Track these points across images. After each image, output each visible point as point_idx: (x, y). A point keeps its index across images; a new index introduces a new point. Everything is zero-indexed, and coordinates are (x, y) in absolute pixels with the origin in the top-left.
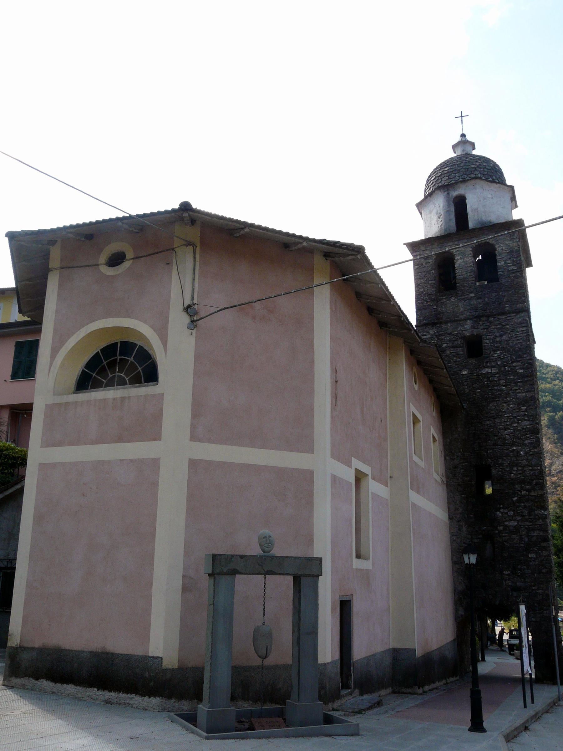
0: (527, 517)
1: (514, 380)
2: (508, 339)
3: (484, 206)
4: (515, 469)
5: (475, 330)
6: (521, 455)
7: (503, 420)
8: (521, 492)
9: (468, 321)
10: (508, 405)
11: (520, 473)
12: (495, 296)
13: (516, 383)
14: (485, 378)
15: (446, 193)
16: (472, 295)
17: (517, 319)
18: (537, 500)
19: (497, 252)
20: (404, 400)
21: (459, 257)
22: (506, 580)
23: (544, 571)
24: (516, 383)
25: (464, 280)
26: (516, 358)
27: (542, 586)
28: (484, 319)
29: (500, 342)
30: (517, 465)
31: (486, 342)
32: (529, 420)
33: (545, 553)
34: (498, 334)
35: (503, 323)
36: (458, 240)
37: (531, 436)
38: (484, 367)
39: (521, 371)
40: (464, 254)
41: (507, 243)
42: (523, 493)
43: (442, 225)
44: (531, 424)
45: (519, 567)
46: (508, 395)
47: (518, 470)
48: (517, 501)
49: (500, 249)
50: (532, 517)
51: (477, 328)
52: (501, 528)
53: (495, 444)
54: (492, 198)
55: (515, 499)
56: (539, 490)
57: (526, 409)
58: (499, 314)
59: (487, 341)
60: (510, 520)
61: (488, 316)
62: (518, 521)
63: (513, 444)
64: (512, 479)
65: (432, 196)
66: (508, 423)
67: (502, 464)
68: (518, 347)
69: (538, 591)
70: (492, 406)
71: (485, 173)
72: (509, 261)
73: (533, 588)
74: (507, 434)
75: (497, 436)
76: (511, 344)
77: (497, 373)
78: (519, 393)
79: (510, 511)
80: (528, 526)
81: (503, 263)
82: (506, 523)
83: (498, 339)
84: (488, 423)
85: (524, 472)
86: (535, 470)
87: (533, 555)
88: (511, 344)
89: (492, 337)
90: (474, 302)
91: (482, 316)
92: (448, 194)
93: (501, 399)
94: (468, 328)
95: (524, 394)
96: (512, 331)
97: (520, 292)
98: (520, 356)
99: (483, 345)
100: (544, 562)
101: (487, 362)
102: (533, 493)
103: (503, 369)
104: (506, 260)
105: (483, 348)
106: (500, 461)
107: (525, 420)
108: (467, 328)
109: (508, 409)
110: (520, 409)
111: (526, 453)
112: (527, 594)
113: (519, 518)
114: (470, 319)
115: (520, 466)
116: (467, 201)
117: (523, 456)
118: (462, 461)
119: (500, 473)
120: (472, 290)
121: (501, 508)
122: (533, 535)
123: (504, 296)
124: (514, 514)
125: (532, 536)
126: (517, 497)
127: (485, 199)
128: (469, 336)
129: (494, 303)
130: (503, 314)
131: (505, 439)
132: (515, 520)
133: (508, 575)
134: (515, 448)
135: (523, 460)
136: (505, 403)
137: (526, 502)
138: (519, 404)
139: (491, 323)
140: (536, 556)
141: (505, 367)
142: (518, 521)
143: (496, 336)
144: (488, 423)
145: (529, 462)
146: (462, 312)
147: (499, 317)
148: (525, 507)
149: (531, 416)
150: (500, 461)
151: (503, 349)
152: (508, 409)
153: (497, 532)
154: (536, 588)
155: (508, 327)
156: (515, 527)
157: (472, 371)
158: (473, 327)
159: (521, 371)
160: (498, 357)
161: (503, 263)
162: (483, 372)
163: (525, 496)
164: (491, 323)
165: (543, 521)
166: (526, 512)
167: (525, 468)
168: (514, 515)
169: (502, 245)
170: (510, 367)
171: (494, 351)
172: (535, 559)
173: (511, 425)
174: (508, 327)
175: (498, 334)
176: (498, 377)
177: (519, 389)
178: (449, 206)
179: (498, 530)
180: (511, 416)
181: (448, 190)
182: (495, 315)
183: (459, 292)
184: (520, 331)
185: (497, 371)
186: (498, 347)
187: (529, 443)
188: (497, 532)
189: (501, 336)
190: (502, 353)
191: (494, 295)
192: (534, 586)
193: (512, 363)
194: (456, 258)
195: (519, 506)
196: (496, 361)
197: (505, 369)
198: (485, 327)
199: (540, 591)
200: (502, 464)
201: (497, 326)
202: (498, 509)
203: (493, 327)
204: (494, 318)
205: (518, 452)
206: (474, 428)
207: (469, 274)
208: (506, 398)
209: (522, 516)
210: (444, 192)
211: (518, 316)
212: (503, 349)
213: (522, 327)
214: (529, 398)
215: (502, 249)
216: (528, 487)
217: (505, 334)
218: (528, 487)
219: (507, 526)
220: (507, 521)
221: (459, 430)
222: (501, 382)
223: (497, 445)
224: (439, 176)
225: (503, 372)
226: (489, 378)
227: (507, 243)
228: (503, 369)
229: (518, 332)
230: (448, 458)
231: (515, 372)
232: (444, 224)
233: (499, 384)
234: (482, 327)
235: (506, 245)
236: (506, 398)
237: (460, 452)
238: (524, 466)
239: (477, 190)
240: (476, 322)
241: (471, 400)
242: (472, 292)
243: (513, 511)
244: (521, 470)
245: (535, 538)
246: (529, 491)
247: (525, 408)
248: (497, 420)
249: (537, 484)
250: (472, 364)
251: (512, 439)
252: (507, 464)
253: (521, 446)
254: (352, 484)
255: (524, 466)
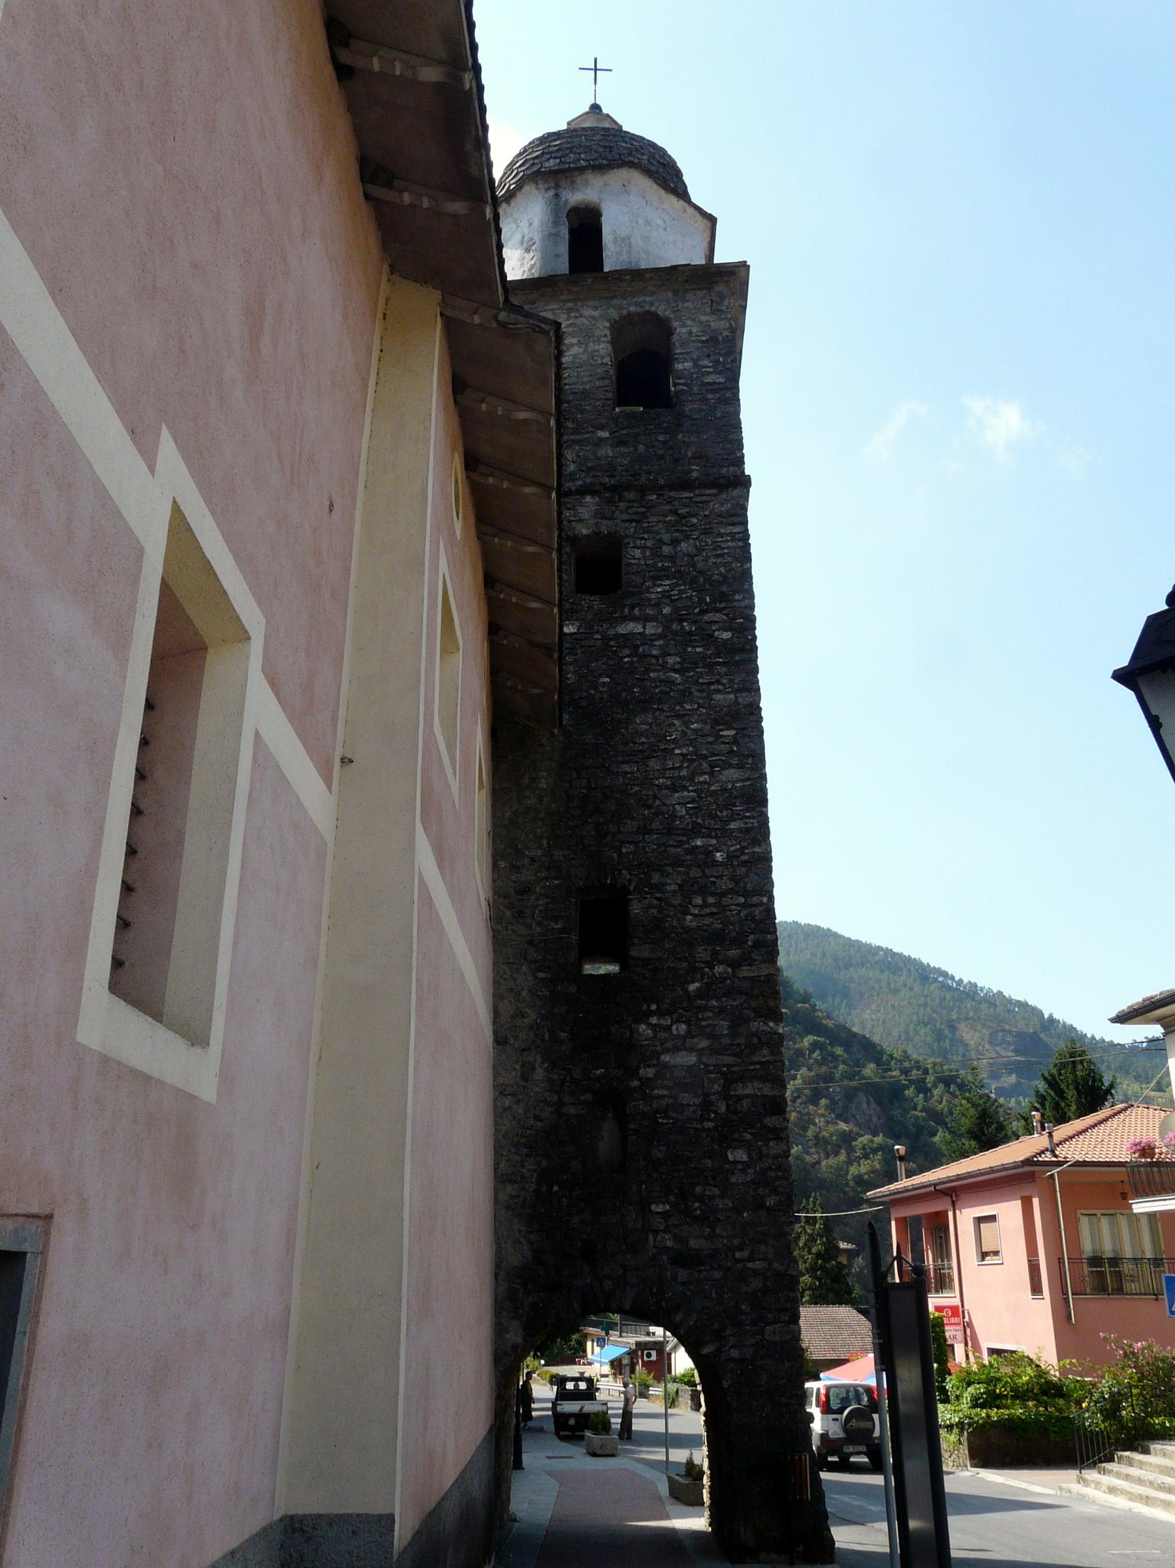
0: (726, 1041)
1: (704, 657)
2: (692, 550)
3: (646, 239)
4: (698, 900)
5: (606, 522)
6: (715, 863)
7: (670, 764)
8: (712, 968)
9: (588, 498)
10: (686, 724)
11: (712, 914)
12: (665, 442)
13: (711, 667)
14: (624, 647)
15: (551, 193)
16: (604, 434)
17: (719, 505)
18: (755, 992)
19: (675, 337)
20: (425, 489)
21: (574, 341)
22: (656, 1232)
23: (770, 1201)
24: (711, 667)
25: (585, 394)
26: (713, 601)
27: (763, 1248)
28: (631, 495)
29: (672, 558)
30: (704, 891)
31: (635, 554)
32: (740, 767)
33: (775, 1148)
34: (666, 538)
35: (682, 511)
36: (575, 300)
37: (748, 810)
38: (625, 619)
39: (726, 635)
40: (587, 335)
41: (704, 318)
42: (719, 969)
43: (533, 266)
44: (748, 779)
45: (698, 1189)
46: (685, 695)
47: (705, 905)
48: (699, 994)
49: (684, 330)
50: (741, 1040)
51: (611, 518)
52: (650, 1072)
53: (645, 830)
54: (665, 229)
55: (693, 987)
56: (764, 962)
57: (734, 737)
58: (672, 487)
59: (638, 553)
60: (676, 1049)
61: (643, 491)
62: (700, 1052)
63: (696, 831)
64: (688, 930)
65: (513, 203)
66: (684, 773)
67: (660, 887)
68: (721, 574)
69: (749, 1265)
70: (641, 722)
71: (653, 168)
72: (706, 362)
73: (737, 1255)
74: (680, 803)
75: (649, 807)
76: (700, 566)
77: (660, 637)
78: (719, 691)
79: (678, 1021)
80: (729, 1066)
81: (688, 365)
82: (666, 1058)
83: (666, 550)
84: (627, 768)
85: (724, 909)
86: (755, 905)
87: (740, 1155)
88: (700, 566)
89: (649, 543)
90: (607, 451)
91: (628, 488)
92: (557, 195)
93: (665, 707)
94: (586, 516)
95: (732, 696)
96: (706, 532)
97: (731, 437)
98: (724, 597)
99: (624, 561)
100: (772, 1174)
101: (632, 607)
102: (745, 972)
103: (675, 626)
104: (699, 359)
105: (624, 571)
106: (656, 878)
107: (731, 766)
108: (586, 517)
109: (684, 733)
110: (718, 737)
111: (730, 857)
112: (717, 1275)
113: (704, 1043)
114: (593, 493)
115: (712, 894)
116: (603, 218)
117: (722, 864)
118: (543, 874)
119: (655, 911)
120: (604, 421)
121: (652, 1013)
122: (740, 1092)
123: (688, 445)
124: (689, 1031)
125: (740, 1098)
126: (701, 980)
127: (648, 222)
128: (587, 536)
129: (662, 458)
130: (686, 485)
131: (674, 816)
132: (691, 1050)
133: (665, 1215)
134: (699, 842)
135: (720, 877)
136: (679, 716)
137: (725, 995)
138: (716, 722)
139: (648, 508)
140: (749, 1156)
141: (681, 621)
142: (700, 1052)
143: (661, 541)
144: (627, 768)
145: (737, 883)
146: (572, 474)
147: (672, 494)
148: (722, 1011)
149: (748, 756)
150: (656, 878)
151: (680, 575)
152: (684, 733)
153: (636, 1083)
154: (746, 1254)
155: (695, 520)
156: (690, 1068)
157: (592, 627)
158: (600, 514)
159: (726, 635)
160: (666, 595)
161: (688, 365)
162: (622, 629)
163: (722, 980)
164: (648, 508)
165: (773, 1054)
166: (724, 1025)
167: (726, 901)
168: (690, 1034)
169: (689, 323)
170: (695, 622)
171: (654, 578)
172: (746, 1165)
173: (691, 778)
174: (695, 520)
175: (666, 538)
176: (661, 647)
177: (718, 682)
178: (556, 223)
179: (640, 1079)
180: (692, 753)
181: (557, 186)
182: (661, 488)
183: (570, 425)
184: (727, 535)
185: (660, 630)
186: (664, 569)
187: (740, 830)
188: (636, 1083)
189: (675, 542)
190: (677, 585)
191: (661, 438)
192: (741, 1248)
193: (703, 612)
194: (566, 342)
195: (702, 1009)
196: (657, 605)
197: (683, 628)
198: (634, 517)
199: (757, 1265)
200: (660, 887)
201: (666, 516)
202: (644, 1017)
203: (654, 519)
204: (659, 496)
205: (708, 853)
206: (585, 781)
207: (597, 383)
208: (681, 704)
209: (712, 1036)
210: (547, 190)
211: (724, 496)
212: (680, 575)
213: (733, 524)
214: (745, 706)
215: (690, 333)
216: (733, 953)
217: (688, 538)
218: (733, 953)
219: (666, 1066)
220: (667, 1051)
221: (543, 785)
222: (671, 660)
223: (651, 832)
224: (537, 157)
225: (676, 633)
226: (637, 647)
227: (704, 318)
228: (675, 626)
229: (721, 535)
230: (502, 864)
231: (708, 638)
232: (538, 265)
233: (664, 666)
234: (626, 517)
235: (701, 322)
236: (681, 704)
237: (540, 847)
238: (723, 894)
239: (632, 197)
240: (610, 501)
241: (583, 703)
242: (602, 428)
243: (688, 1022)
244: (713, 905)
245: (745, 1103)
246: (735, 964)
247: (732, 732)
248: (654, 764)
249: (757, 945)
250: (590, 608)
251: (691, 816)
252: (674, 887)
253: (716, 837)
254: (139, 552)
255: (723, 894)
